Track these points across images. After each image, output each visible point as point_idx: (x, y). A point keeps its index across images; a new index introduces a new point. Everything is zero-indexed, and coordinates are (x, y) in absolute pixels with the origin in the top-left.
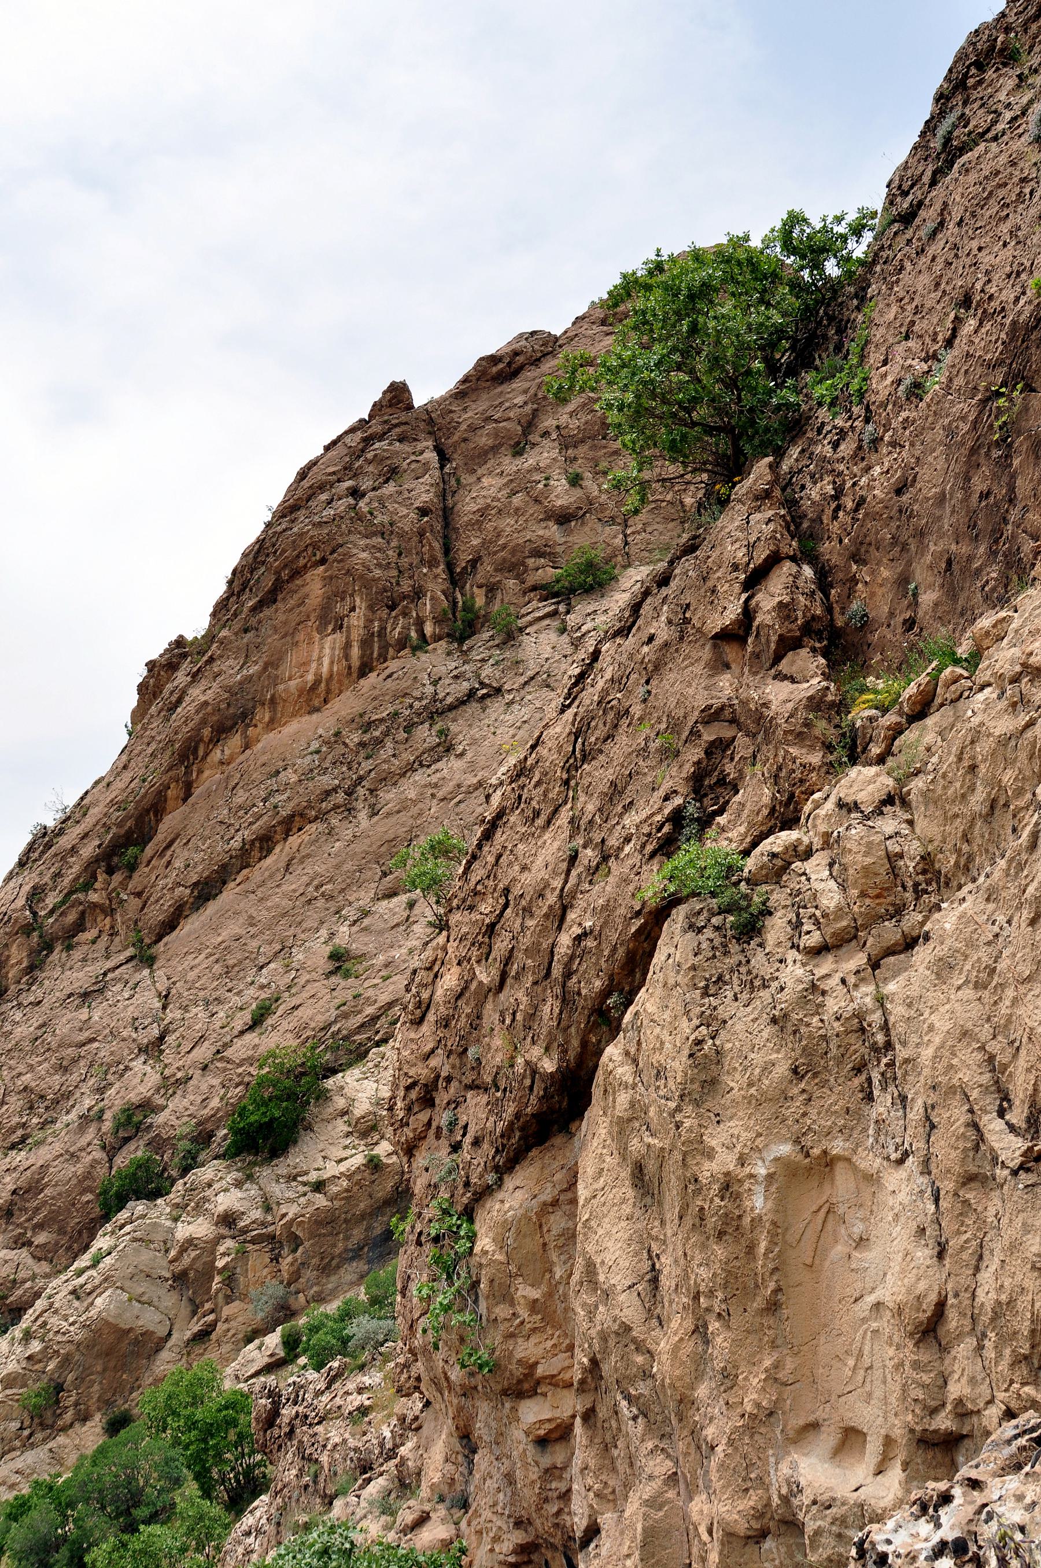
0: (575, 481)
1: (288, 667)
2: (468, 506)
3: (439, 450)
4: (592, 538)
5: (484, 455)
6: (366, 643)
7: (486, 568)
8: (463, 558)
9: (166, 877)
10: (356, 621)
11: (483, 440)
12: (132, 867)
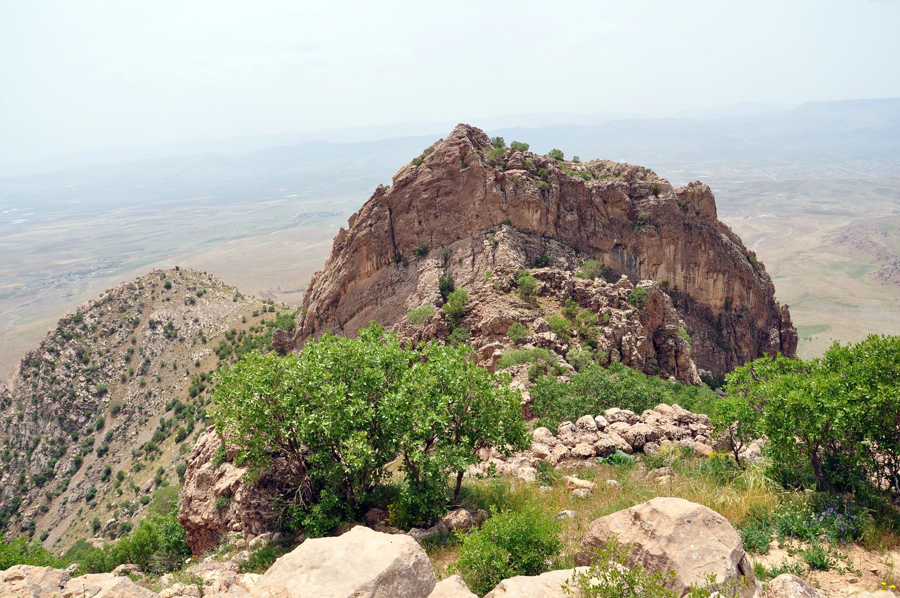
0: (420, 222)
1: (361, 269)
2: (397, 228)
3: (390, 210)
4: (426, 239)
5: (400, 213)
6: (377, 264)
7: (401, 245)
8: (397, 243)
9: (343, 311)
10: (374, 259)
11: (399, 208)
12: (336, 307)
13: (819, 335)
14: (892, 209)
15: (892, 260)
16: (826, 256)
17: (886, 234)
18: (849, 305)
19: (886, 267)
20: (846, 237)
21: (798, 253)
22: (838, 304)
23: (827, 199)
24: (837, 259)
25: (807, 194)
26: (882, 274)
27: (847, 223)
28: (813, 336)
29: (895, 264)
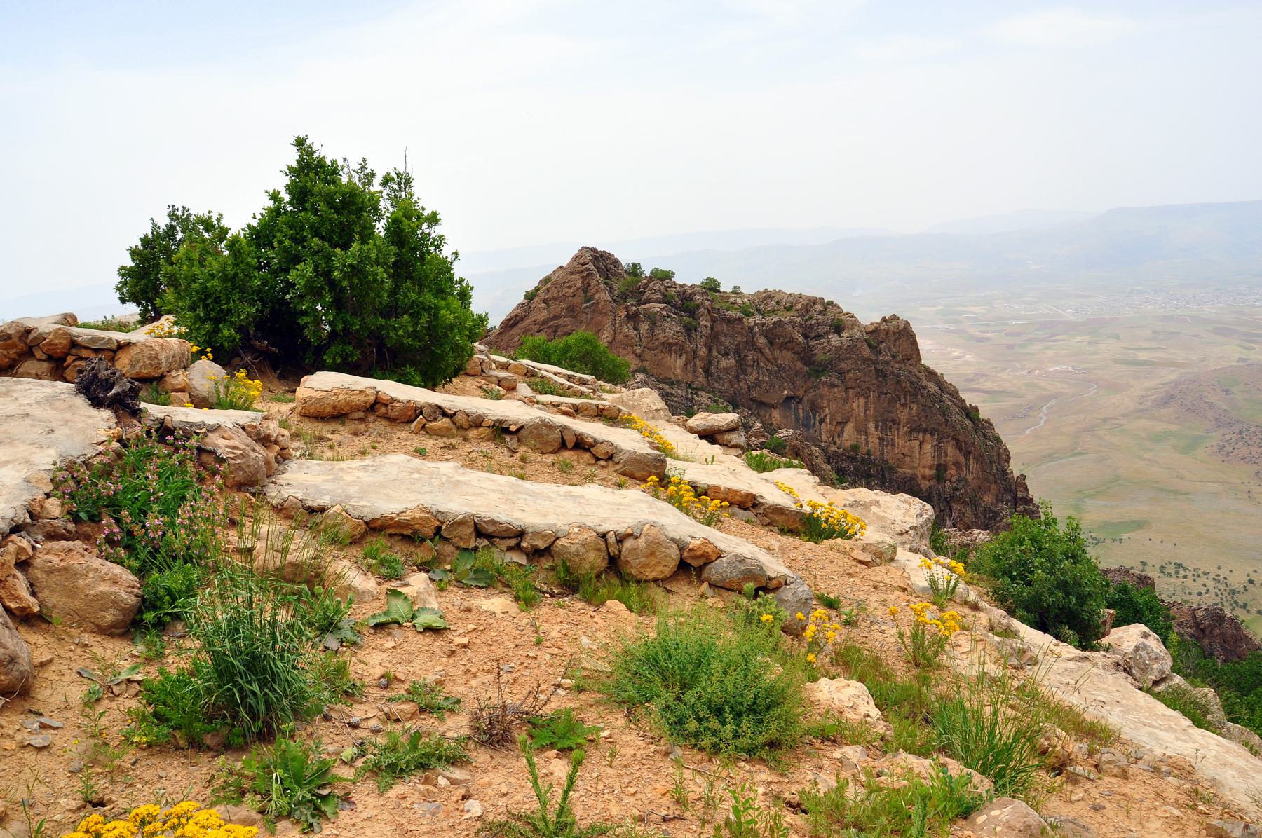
13: (1132, 534)
14: (1237, 356)
15: (1236, 428)
16: (1143, 423)
17: (1227, 392)
18: (1176, 492)
19: (1228, 437)
20: (1172, 397)
21: (1105, 420)
22: (1161, 490)
23: (1145, 345)
24: (1159, 427)
25: (1117, 337)
26: (1222, 448)
27: (1173, 376)
28: (1125, 536)
29: (1240, 433)
